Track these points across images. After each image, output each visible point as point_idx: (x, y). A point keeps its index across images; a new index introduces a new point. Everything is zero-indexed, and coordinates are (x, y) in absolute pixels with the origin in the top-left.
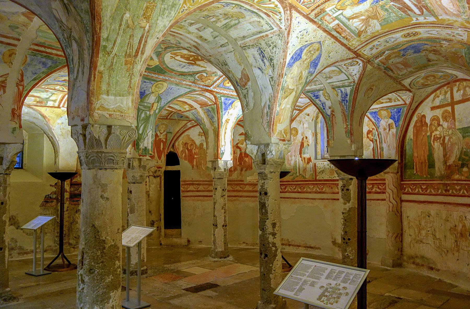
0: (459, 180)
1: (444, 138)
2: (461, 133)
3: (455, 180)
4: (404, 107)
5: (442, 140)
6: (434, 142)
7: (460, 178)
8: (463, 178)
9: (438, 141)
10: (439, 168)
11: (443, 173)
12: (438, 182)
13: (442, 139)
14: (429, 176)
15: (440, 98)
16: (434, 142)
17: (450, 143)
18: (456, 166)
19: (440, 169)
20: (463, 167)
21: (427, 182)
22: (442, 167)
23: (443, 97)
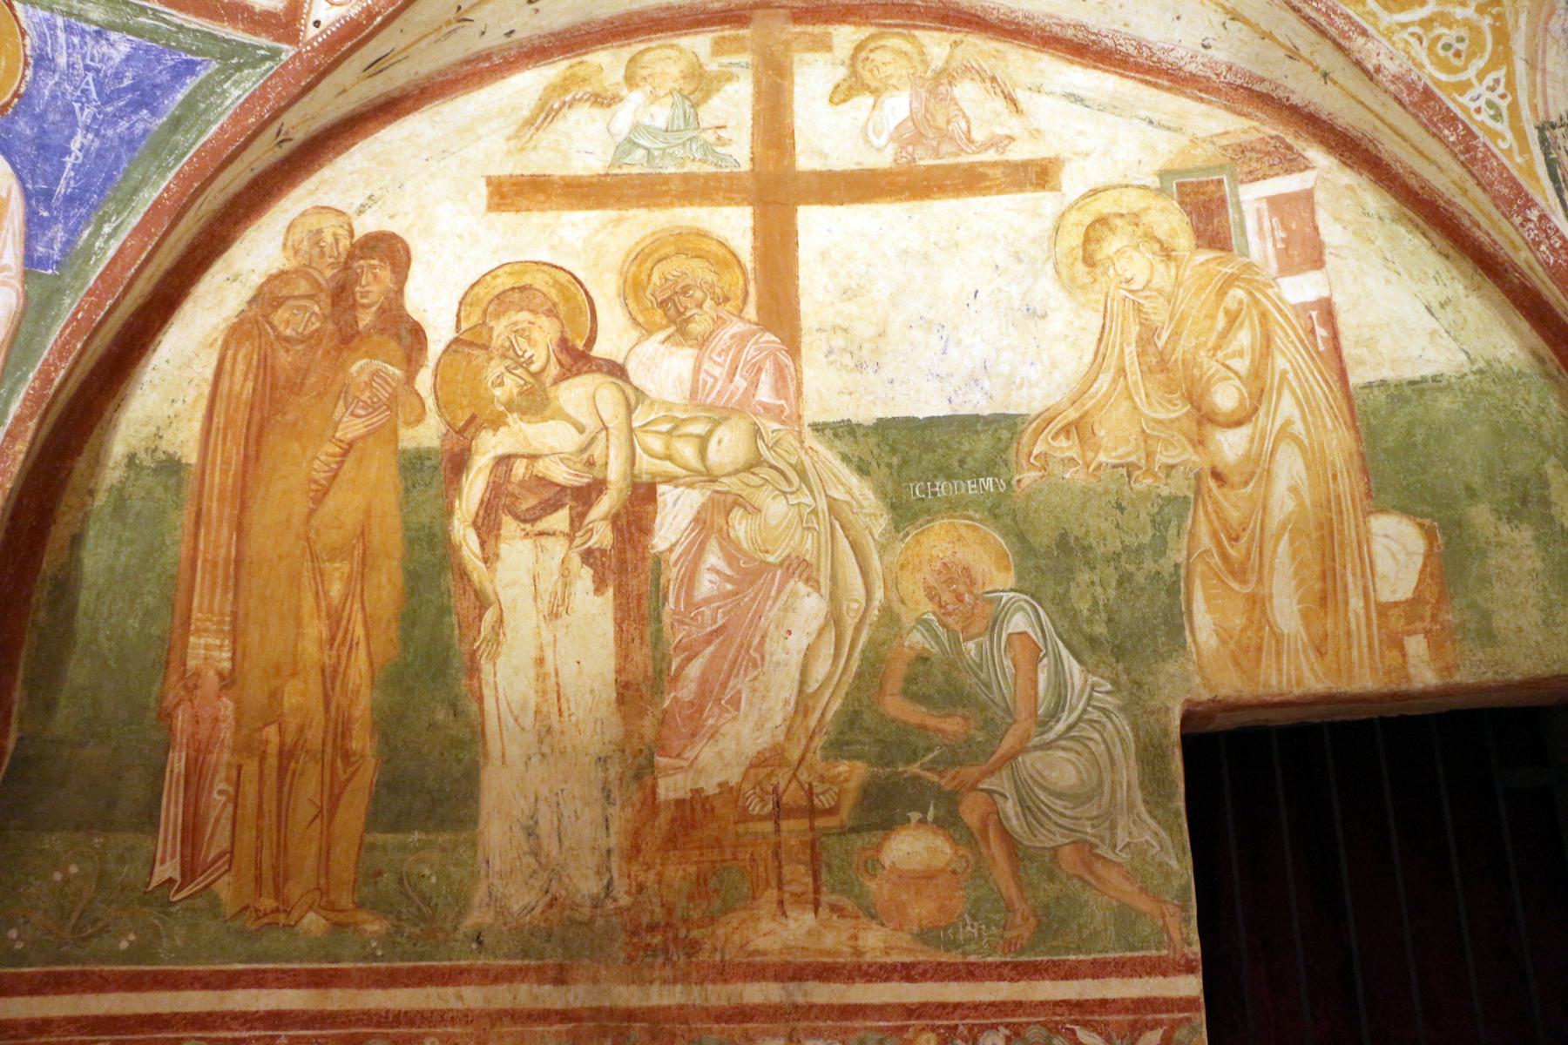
0: (826, 972)
1: (643, 495)
2: (862, 470)
3: (756, 972)
4: (235, 58)
5: (615, 519)
6: (487, 525)
7: (829, 940)
8: (874, 942)
9: (559, 520)
10: (531, 833)
11: (589, 886)
12: (503, 996)
13: (605, 505)
14: (374, 926)
15: (624, 117)
16: (487, 525)
17: (713, 558)
18: (779, 812)
19: (550, 846)
20: (888, 825)
21: (337, 1000)
22: (591, 814)
23: (660, 115)
